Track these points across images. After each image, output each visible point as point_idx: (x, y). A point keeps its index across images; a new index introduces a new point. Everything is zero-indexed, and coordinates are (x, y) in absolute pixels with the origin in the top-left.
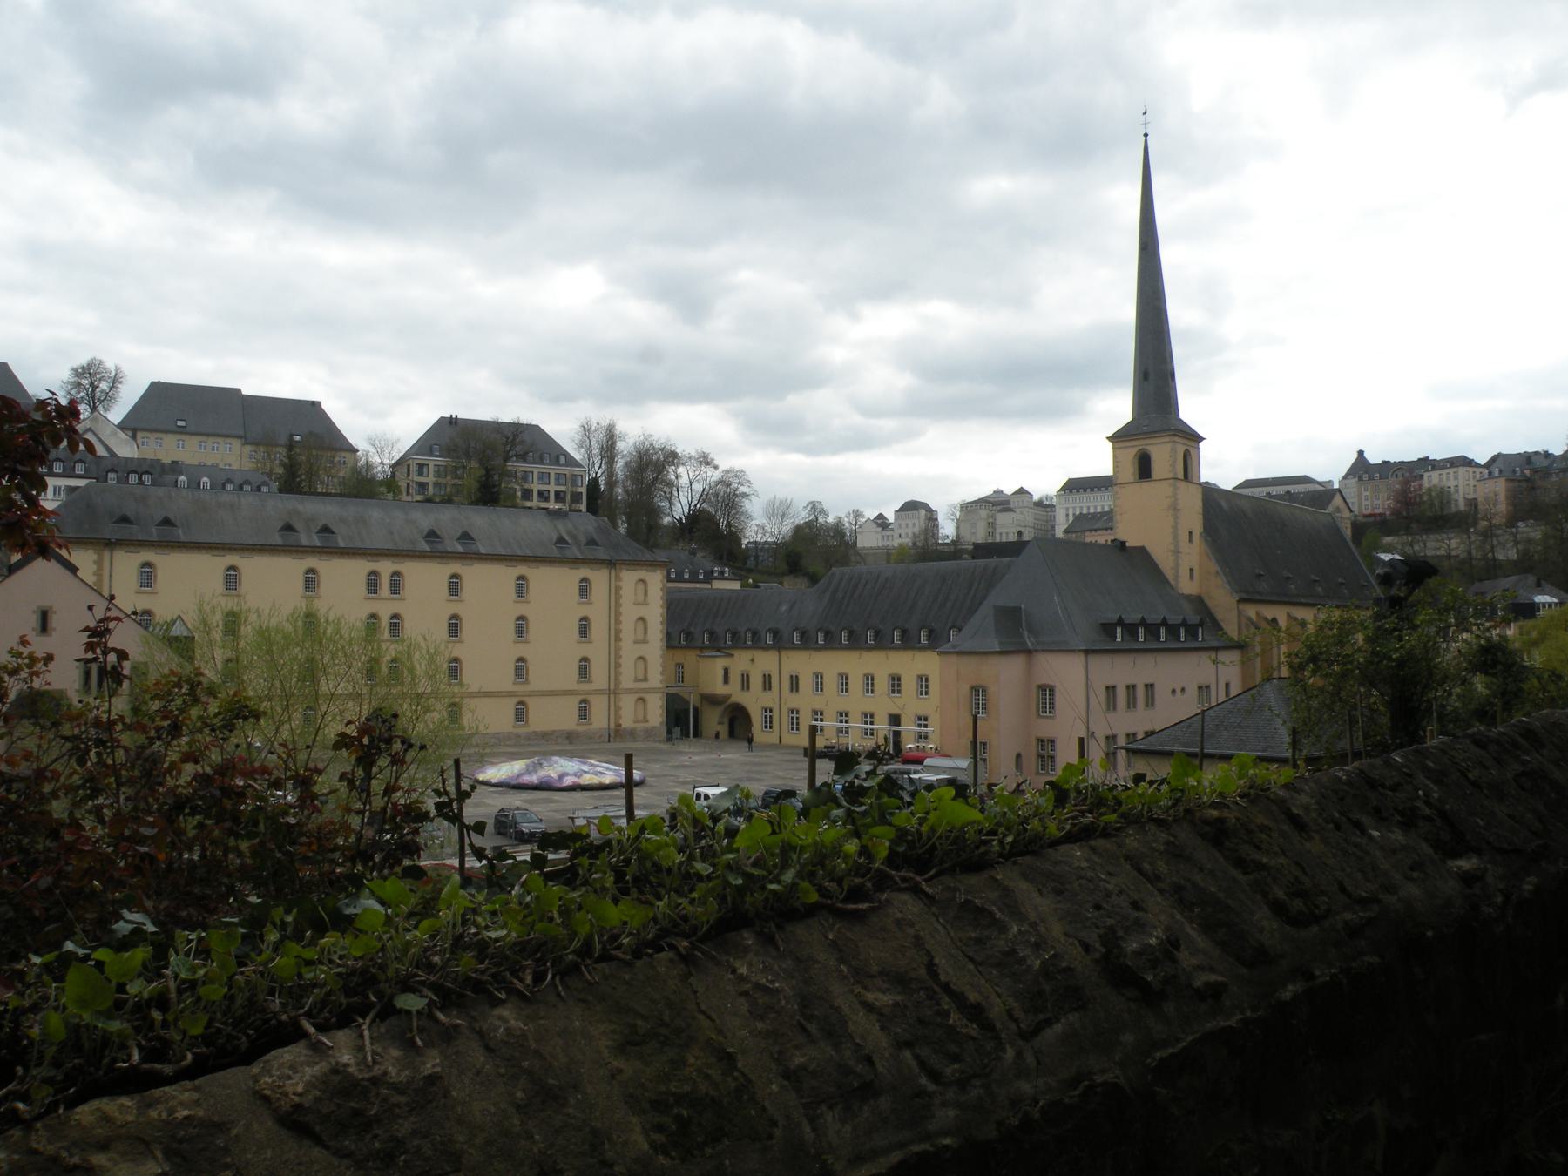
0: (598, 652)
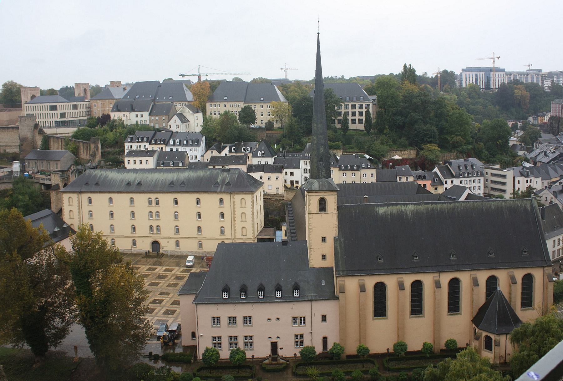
0: (227, 224)
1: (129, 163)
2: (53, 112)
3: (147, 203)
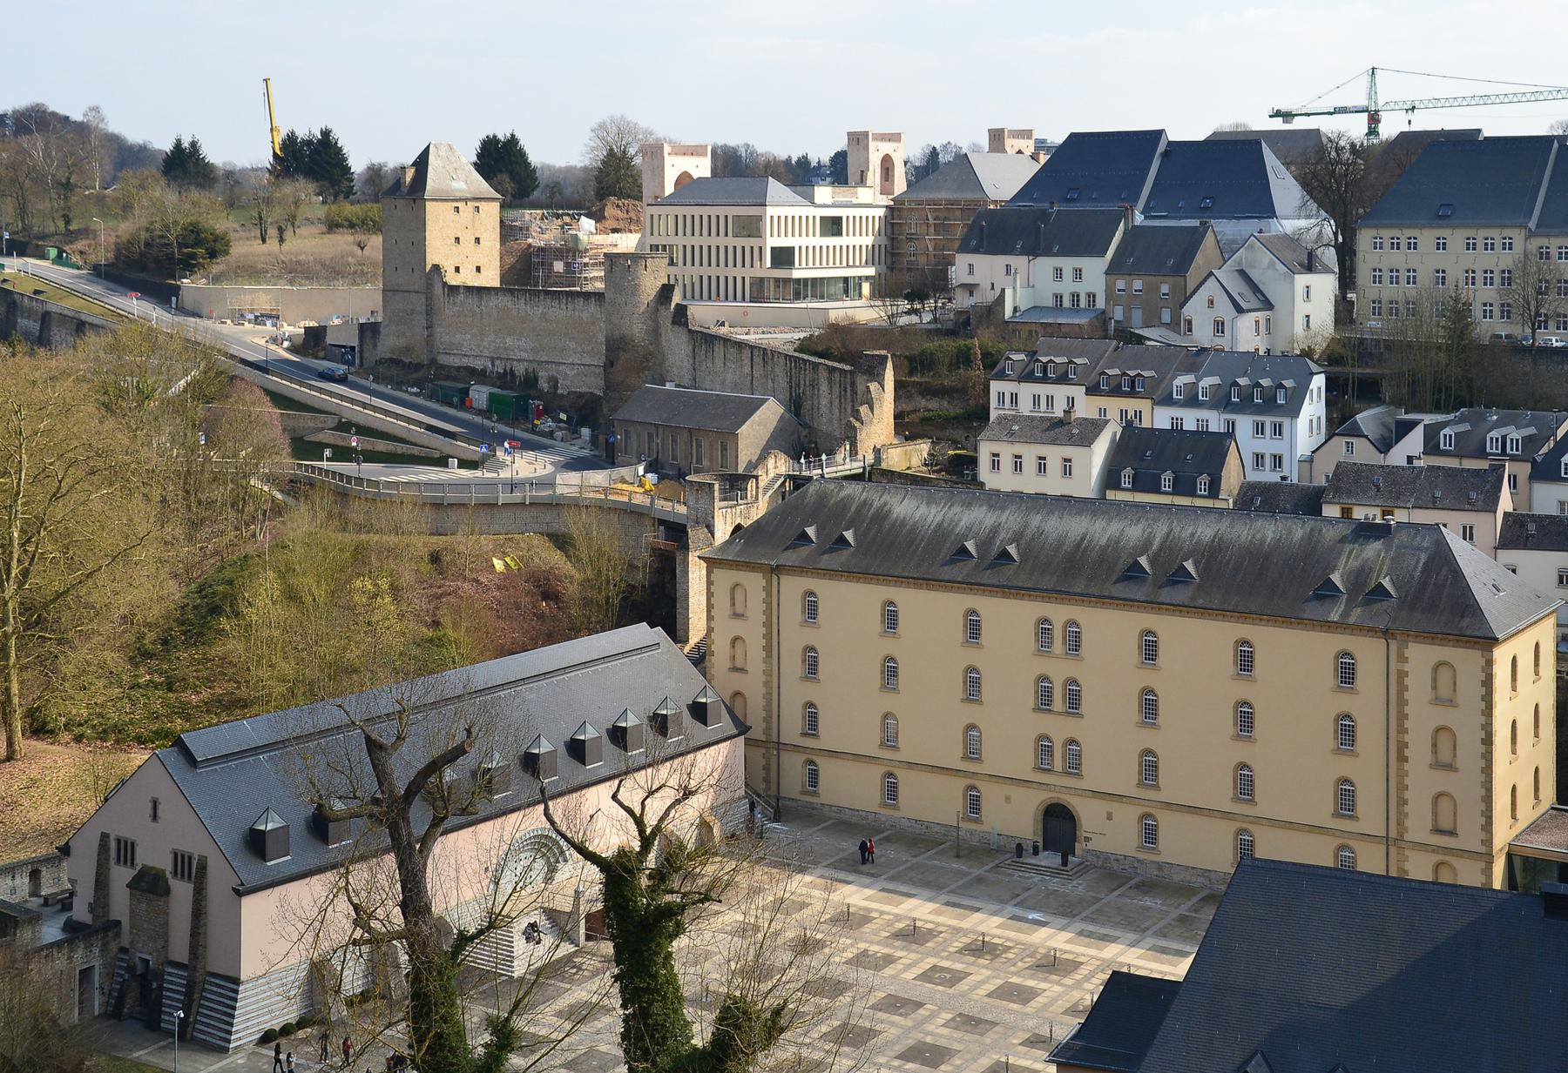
1: (995, 465)
2: (748, 242)
3: (1029, 641)
